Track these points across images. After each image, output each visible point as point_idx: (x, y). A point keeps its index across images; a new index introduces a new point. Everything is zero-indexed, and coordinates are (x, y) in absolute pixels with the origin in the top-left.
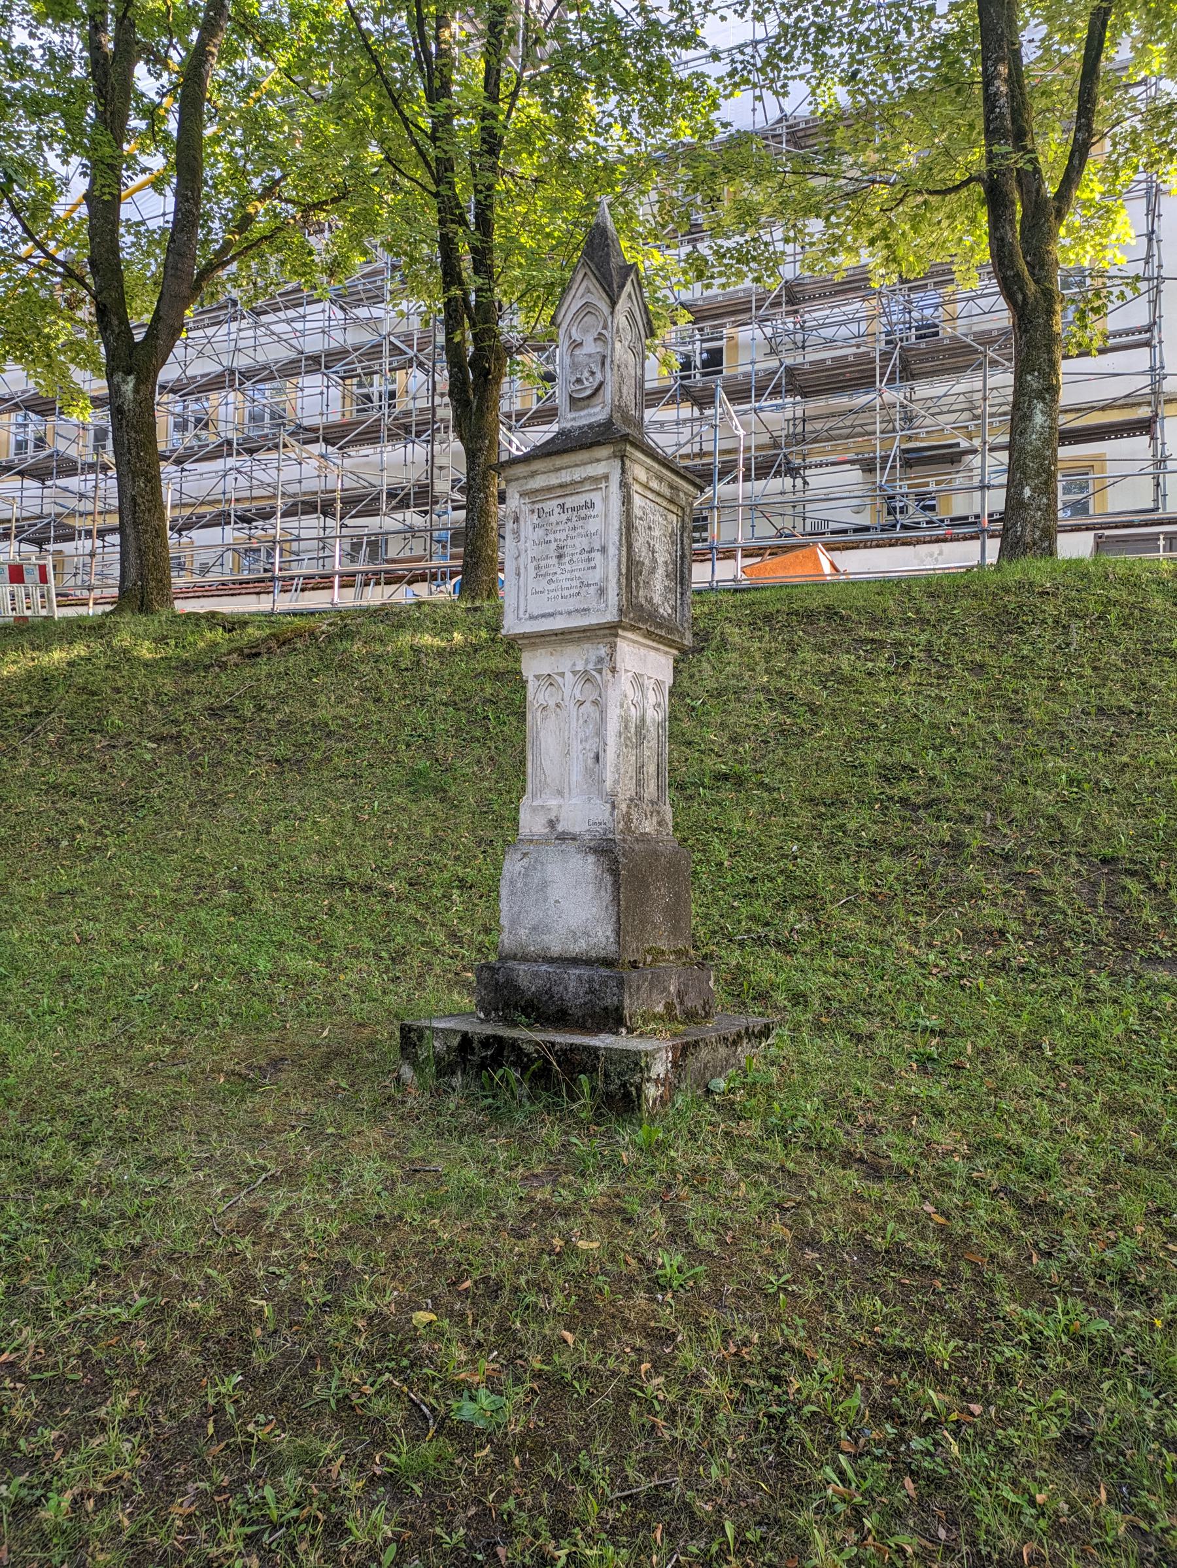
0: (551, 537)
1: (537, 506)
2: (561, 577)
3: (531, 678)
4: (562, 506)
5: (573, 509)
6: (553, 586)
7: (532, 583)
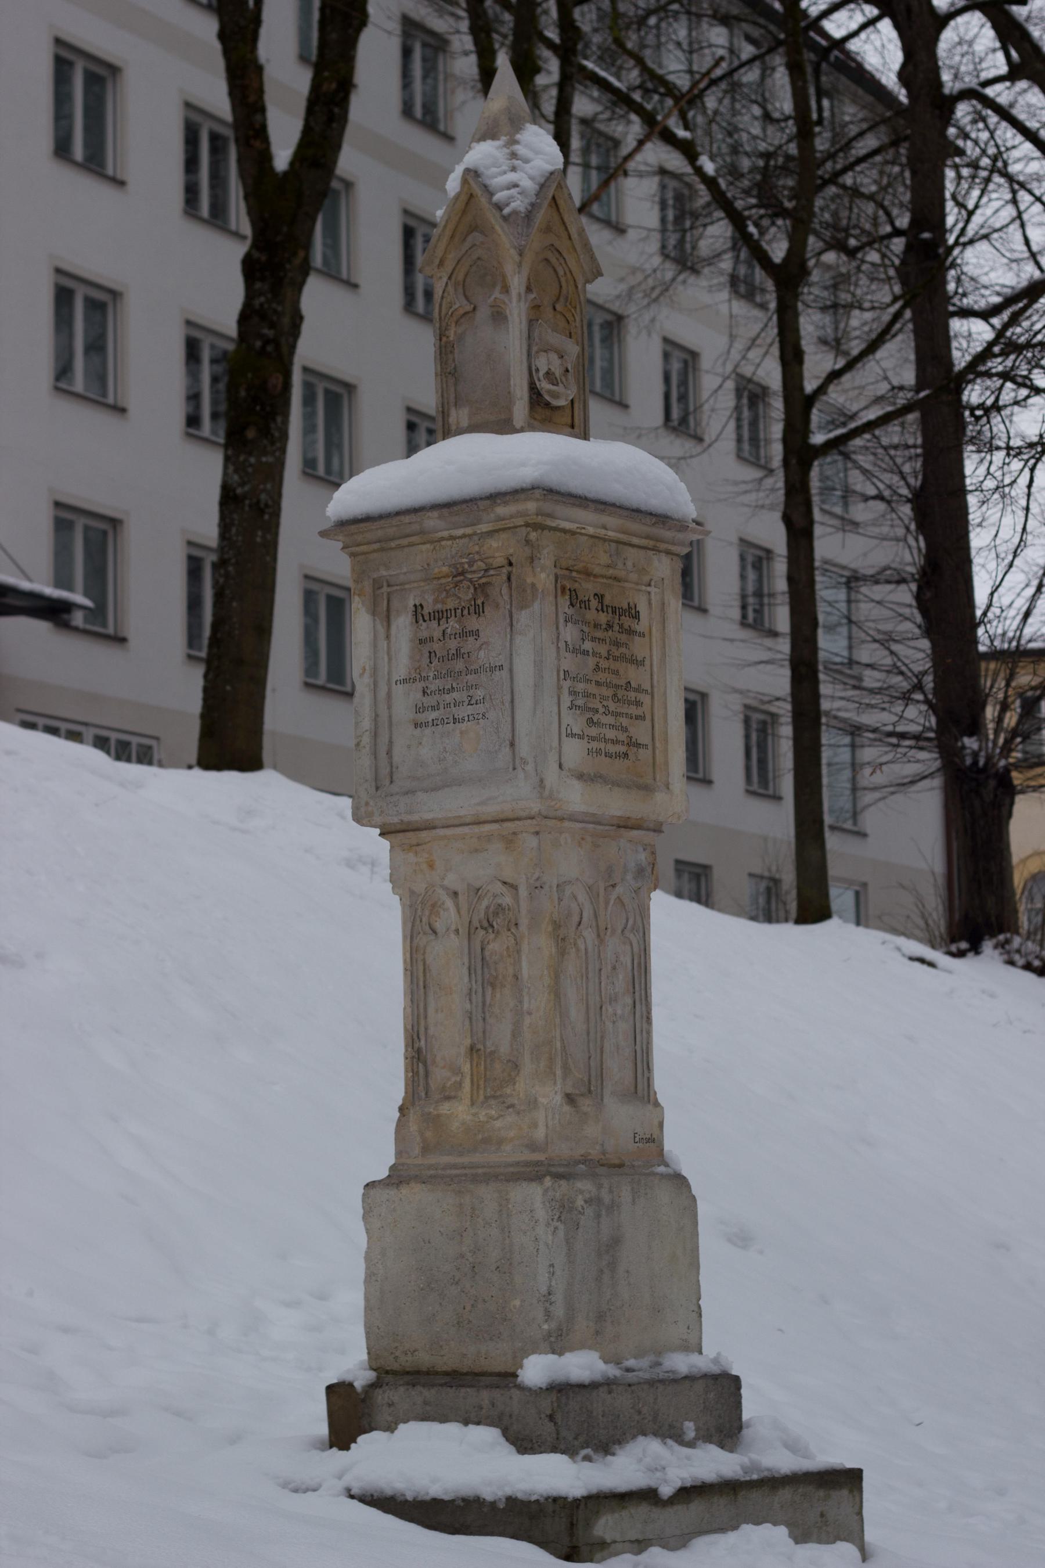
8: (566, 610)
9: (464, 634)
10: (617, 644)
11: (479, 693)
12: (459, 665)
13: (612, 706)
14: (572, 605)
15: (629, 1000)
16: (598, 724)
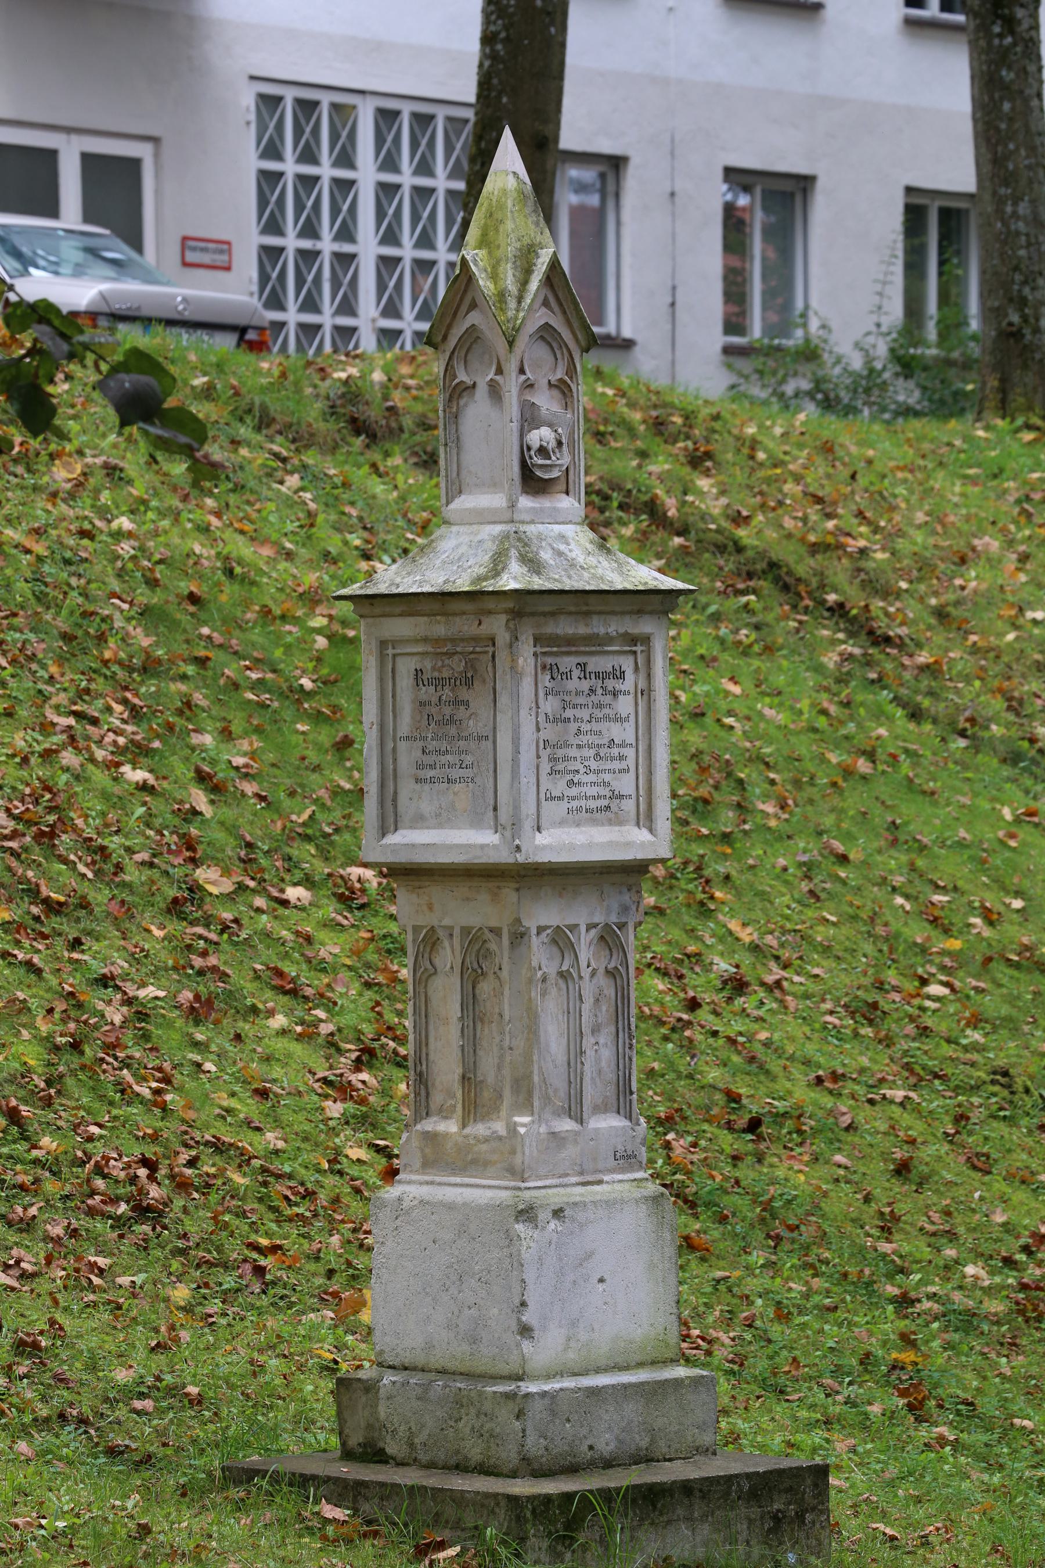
0: (569, 713)
1: (549, 660)
2: (585, 779)
5: (597, 675)
6: (574, 791)
7: (546, 783)
9: (457, 702)
10: (600, 706)
11: (468, 759)
12: (453, 731)
13: (594, 765)
15: (613, 1029)
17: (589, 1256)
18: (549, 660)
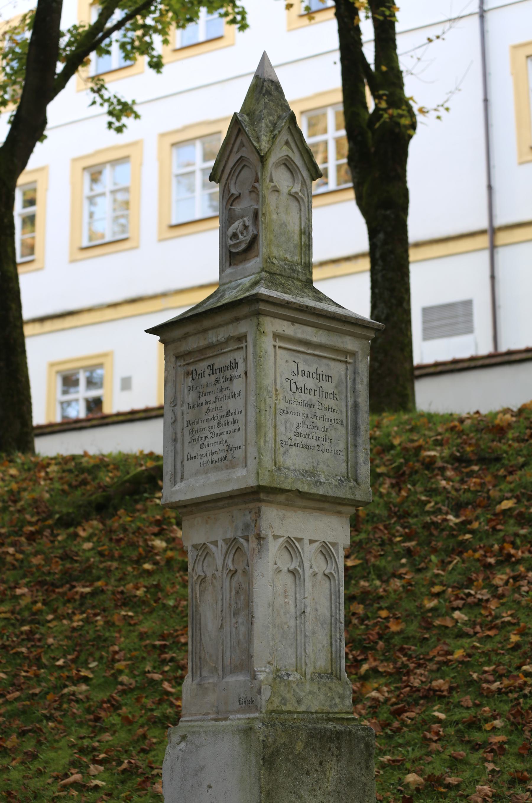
0: (202, 400)
1: (191, 368)
2: (211, 441)
3: (190, 549)
4: (211, 367)
5: (220, 370)
6: (204, 451)
8: (190, 384)
13: (216, 430)
14: (193, 379)
16: (208, 445)
17: (202, 769)
18: (191, 368)
